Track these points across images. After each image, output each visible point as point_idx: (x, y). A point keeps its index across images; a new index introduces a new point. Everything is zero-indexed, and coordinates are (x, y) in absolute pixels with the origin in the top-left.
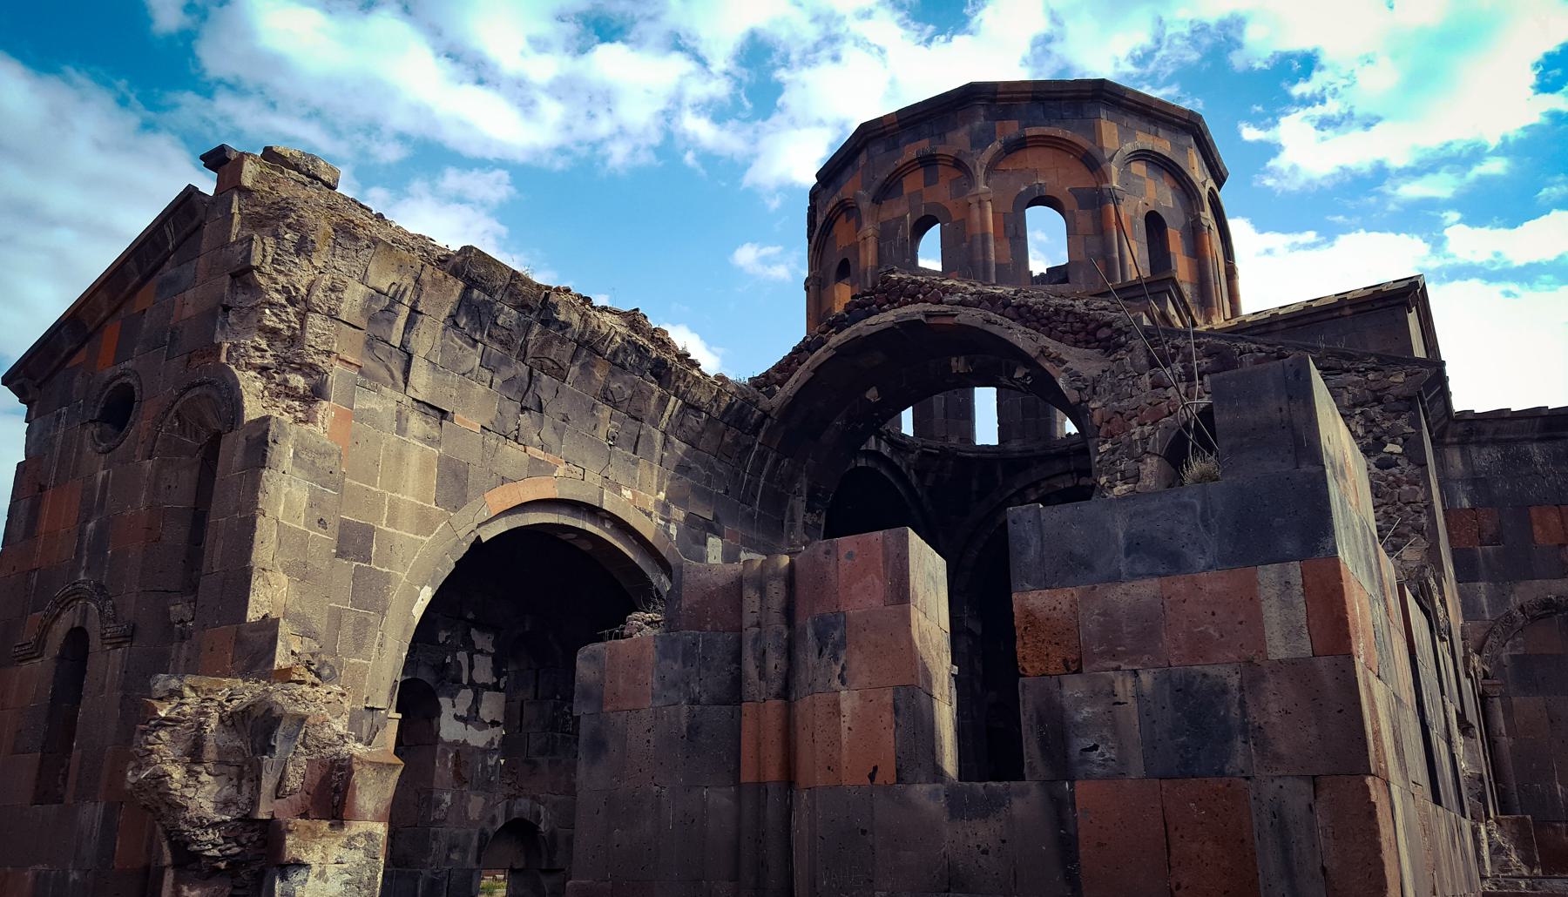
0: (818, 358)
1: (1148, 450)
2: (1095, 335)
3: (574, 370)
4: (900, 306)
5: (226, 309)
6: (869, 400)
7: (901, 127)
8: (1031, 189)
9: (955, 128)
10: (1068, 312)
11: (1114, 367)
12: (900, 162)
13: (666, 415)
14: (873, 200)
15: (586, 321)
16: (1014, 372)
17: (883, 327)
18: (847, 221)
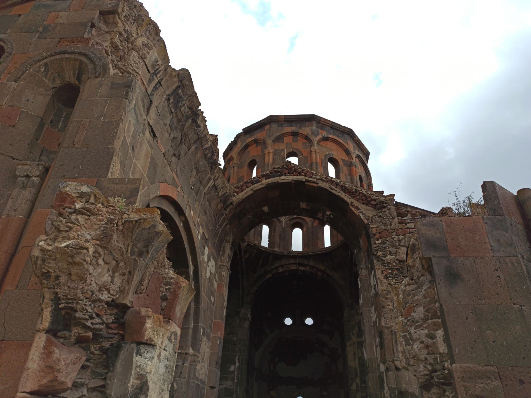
0: (257, 187)
1: (401, 244)
2: (370, 202)
3: (193, 148)
4: (294, 175)
5: (93, 26)
6: (264, 211)
7: (285, 121)
8: (329, 154)
9: (305, 127)
10: (360, 193)
11: (380, 214)
12: (285, 131)
13: (209, 186)
14: (273, 141)
15: (205, 129)
16: (326, 212)
17: (288, 181)
18: (256, 147)
